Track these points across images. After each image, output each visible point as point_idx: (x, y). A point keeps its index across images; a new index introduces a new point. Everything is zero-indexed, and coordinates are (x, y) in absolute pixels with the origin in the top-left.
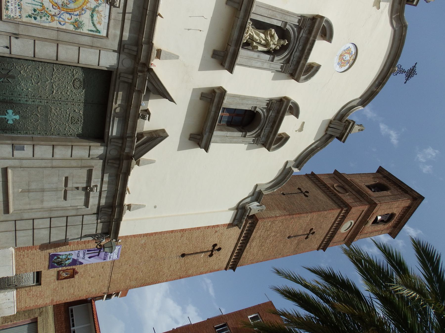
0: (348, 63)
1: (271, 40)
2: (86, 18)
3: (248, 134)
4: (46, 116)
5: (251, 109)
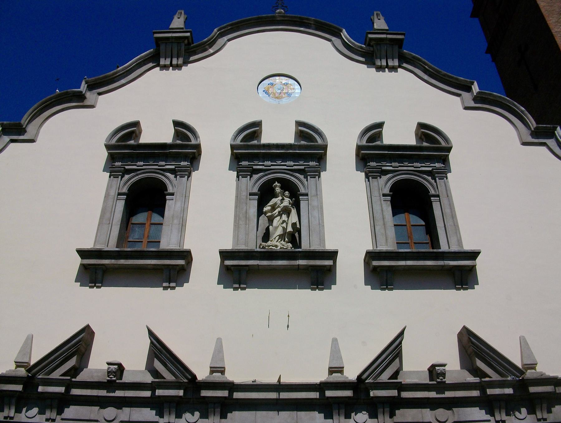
1: (279, 207)
3: (432, 192)
5: (389, 203)
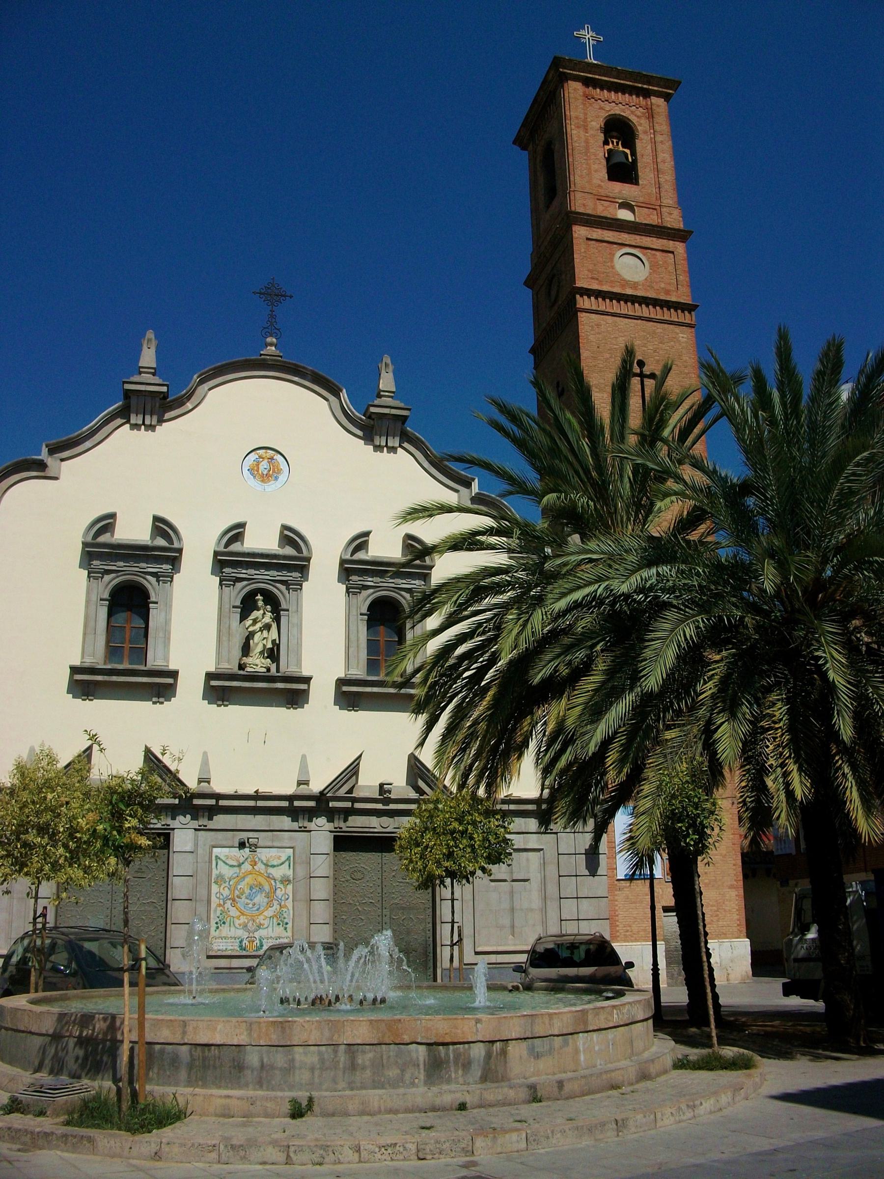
0: (272, 458)
2: (277, 873)
4: (403, 908)
5: (365, 622)
